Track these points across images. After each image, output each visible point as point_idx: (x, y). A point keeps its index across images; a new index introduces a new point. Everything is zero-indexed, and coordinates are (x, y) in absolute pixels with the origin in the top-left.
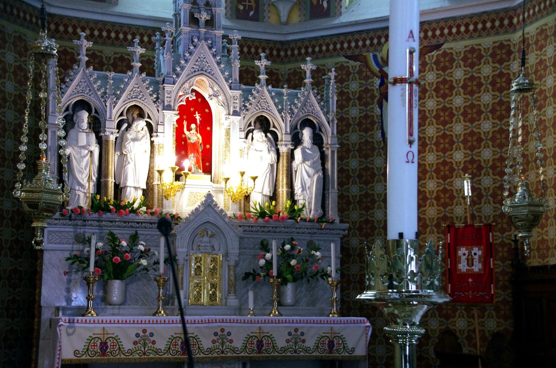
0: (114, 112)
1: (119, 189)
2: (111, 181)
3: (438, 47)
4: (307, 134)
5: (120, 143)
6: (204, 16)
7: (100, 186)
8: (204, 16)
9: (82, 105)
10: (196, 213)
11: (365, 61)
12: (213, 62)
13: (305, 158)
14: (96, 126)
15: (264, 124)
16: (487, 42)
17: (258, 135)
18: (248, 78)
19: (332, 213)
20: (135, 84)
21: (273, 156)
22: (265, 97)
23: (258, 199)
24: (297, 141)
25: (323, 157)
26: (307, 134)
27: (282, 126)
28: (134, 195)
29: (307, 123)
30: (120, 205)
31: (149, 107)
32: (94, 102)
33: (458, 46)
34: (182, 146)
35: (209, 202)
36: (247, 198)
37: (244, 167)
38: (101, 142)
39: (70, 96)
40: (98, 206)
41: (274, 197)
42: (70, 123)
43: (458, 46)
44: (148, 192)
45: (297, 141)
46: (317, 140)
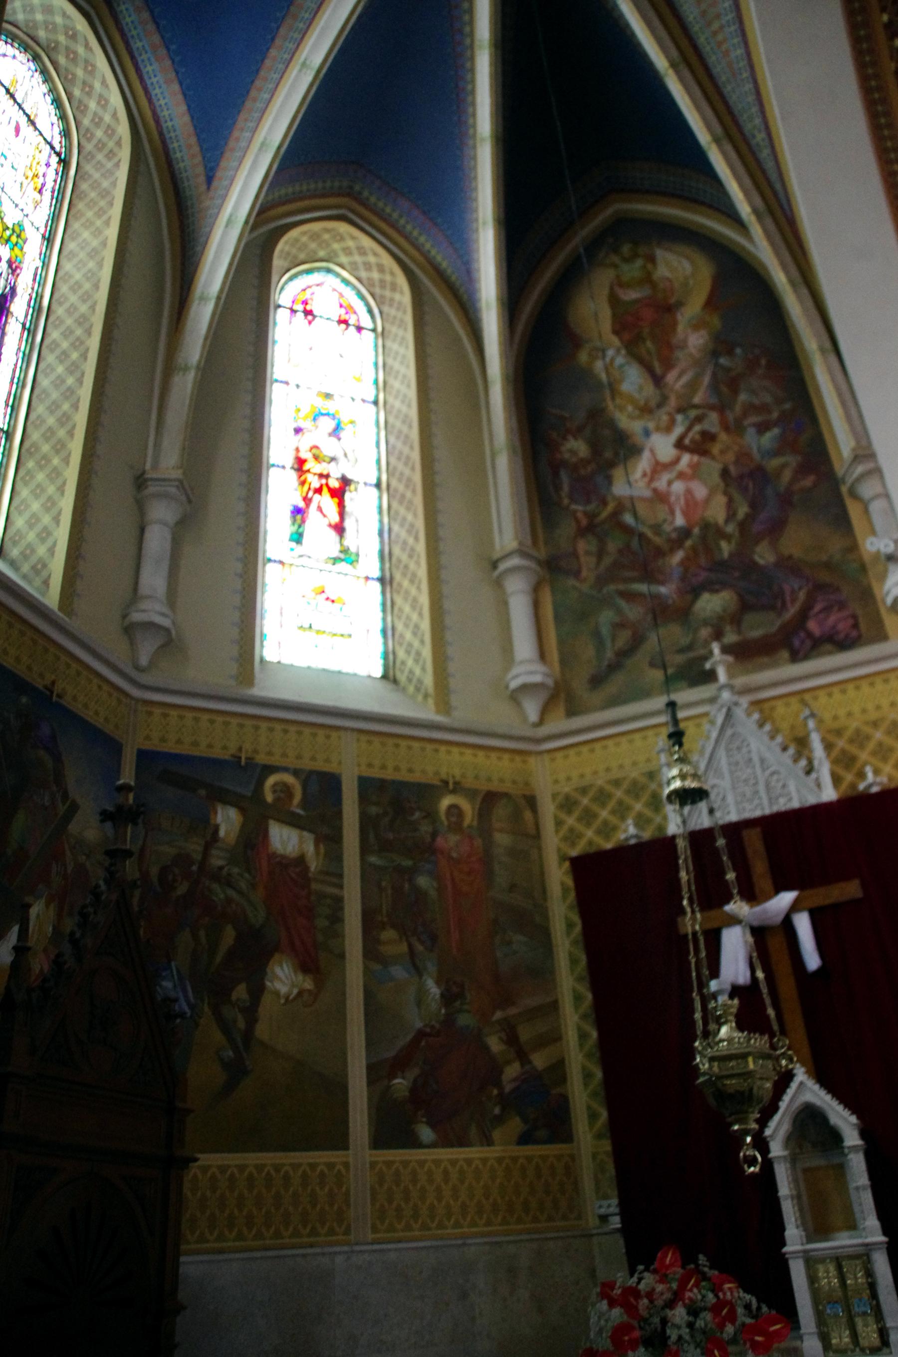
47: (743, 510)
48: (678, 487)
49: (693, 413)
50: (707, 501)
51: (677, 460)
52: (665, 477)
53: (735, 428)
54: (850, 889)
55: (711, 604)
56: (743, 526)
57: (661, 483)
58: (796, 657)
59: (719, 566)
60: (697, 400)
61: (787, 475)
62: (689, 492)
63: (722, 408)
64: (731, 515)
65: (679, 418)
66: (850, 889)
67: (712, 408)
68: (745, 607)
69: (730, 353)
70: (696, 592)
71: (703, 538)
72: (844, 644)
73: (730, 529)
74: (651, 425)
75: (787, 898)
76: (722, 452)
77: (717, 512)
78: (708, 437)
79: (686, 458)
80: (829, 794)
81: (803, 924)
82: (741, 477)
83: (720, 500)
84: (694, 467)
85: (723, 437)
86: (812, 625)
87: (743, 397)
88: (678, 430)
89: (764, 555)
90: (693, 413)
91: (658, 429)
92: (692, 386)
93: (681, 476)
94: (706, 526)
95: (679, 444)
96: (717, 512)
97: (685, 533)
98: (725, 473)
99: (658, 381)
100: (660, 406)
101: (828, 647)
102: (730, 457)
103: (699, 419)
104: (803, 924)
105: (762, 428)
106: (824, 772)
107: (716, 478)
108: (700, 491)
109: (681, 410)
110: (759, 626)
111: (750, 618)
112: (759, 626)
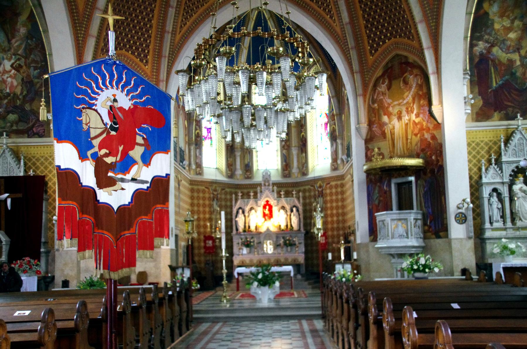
0: (247, 209)
1: (249, 227)
2: (247, 225)
3: (329, 184)
4: (294, 209)
5: (248, 216)
6: (267, 184)
7: (245, 226)
8: (267, 184)
9: (240, 208)
10: (265, 232)
11: (314, 187)
12: (269, 195)
13: (294, 215)
14: (243, 212)
15: (283, 208)
16: (339, 183)
17: (282, 211)
18: (279, 196)
19: (302, 229)
20: (251, 202)
21: (285, 216)
22: (284, 201)
23: (283, 227)
24: (292, 211)
25: (299, 214)
26: (294, 209)
27: (288, 208)
28: (253, 228)
29: (294, 206)
30: (250, 231)
31: (255, 207)
32: (243, 207)
33: (333, 183)
34: (265, 215)
35: (268, 229)
36: (280, 226)
37: (280, 219)
38: (245, 216)
39: (238, 206)
40: (244, 231)
41: (287, 226)
42: (238, 212)
43: (333, 183)
44: (256, 227)
45: (292, 211)
46: (298, 210)
47: (25, 93)
48: (9, 80)
49: (18, 57)
50: (16, 86)
51: (10, 71)
52: (7, 75)
53: (29, 67)
54: (20, 195)
55: (12, 117)
56: (24, 97)
57: (5, 77)
58: (29, 137)
59: (16, 107)
60: (19, 52)
61: (38, 85)
62: (12, 82)
63: (26, 58)
64: (22, 93)
65: (13, 57)
66: (20, 195)
67: (23, 57)
68: (20, 120)
69: (32, 40)
70: (8, 113)
71: (13, 98)
72: (41, 136)
73: (21, 97)
74: (5, 56)
75: (7, 195)
76: (23, 73)
77: (18, 91)
78: (20, 66)
79: (13, 71)
80: (22, 174)
81: (9, 201)
82: (27, 82)
83: (20, 88)
84: (15, 75)
85: (24, 67)
86: (34, 129)
87: (32, 56)
88: (13, 61)
89: (27, 107)
90: (18, 57)
91: (7, 59)
92: (19, 47)
93: (11, 76)
94: (15, 94)
95: (12, 66)
96: (18, 91)
97: (9, 94)
98: (23, 80)
99: (9, 41)
100: (8, 51)
101: (37, 136)
102: (25, 75)
103: (19, 59)
104: (9, 201)
105: (35, 68)
106: (22, 169)
107: (20, 81)
108: (15, 83)
109: (14, 54)
110: (22, 126)
111: (20, 124)
112: (22, 126)
